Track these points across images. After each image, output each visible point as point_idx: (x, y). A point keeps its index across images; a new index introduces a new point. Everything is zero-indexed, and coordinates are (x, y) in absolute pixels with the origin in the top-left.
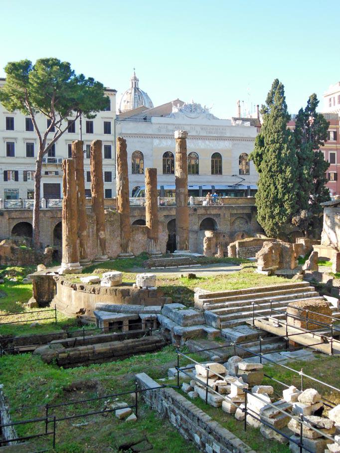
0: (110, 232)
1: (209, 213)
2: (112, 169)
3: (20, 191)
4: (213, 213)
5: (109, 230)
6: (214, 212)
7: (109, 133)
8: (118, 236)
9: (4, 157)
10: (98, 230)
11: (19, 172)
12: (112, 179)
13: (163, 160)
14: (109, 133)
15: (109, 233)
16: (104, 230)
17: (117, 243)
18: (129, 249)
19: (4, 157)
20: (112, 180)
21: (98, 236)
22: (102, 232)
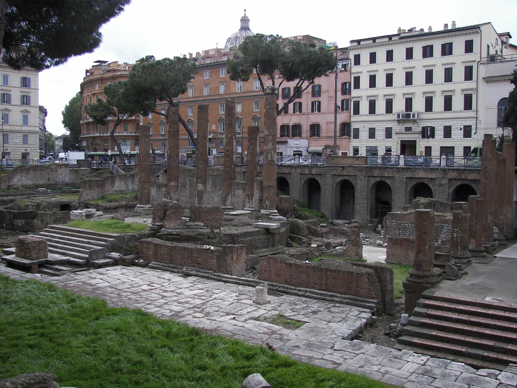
0: (212, 185)
1: (463, 177)
2: (473, 122)
3: (379, 148)
4: (469, 178)
5: (210, 183)
6: (471, 176)
7: (471, 79)
8: (220, 190)
9: (367, 115)
10: (197, 183)
11: (436, 128)
12: (472, 134)
13: (498, 109)
14: (471, 79)
15: (210, 186)
16: (204, 183)
17: (219, 195)
18: (228, 202)
19: (367, 115)
20: (472, 136)
21: (196, 188)
22: (200, 185)
